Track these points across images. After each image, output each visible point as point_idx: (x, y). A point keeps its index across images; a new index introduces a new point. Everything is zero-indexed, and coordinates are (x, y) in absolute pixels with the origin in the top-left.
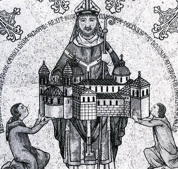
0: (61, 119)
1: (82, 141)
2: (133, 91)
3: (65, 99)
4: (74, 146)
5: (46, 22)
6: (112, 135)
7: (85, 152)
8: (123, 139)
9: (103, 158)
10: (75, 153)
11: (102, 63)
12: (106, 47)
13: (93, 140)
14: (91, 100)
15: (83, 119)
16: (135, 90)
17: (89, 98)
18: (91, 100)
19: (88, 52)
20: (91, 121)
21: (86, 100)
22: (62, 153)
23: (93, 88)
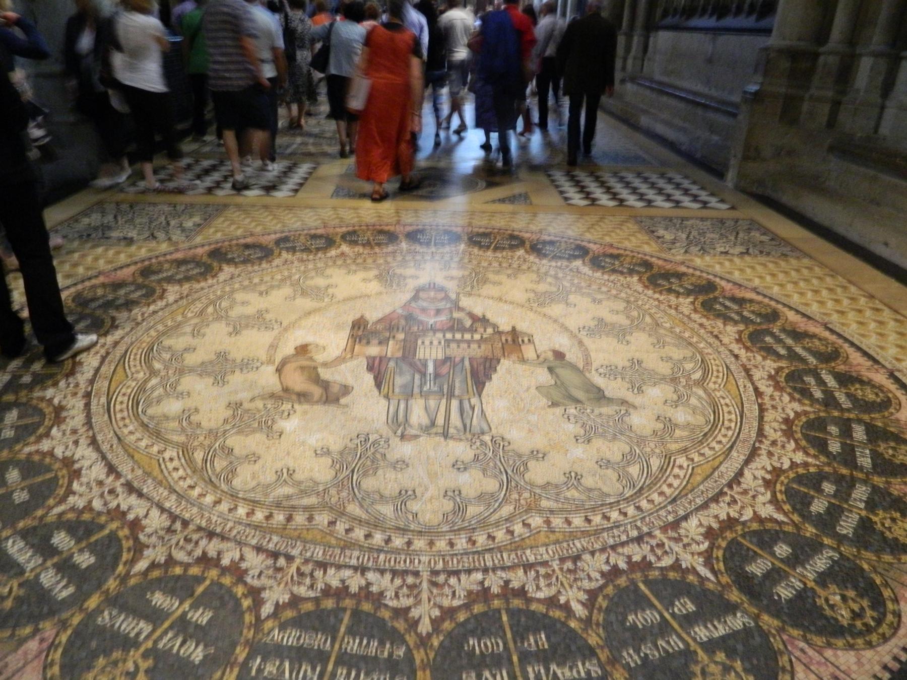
0: (381, 358)
1: (417, 377)
2: (507, 340)
3: (391, 342)
4: (399, 381)
5: (373, 292)
6: (474, 374)
7: (421, 386)
8: (494, 377)
9: (457, 392)
10: (404, 386)
11: (451, 318)
12: (460, 309)
13: (437, 375)
14: (435, 343)
15: (422, 357)
16: (510, 339)
17: (431, 343)
18: (435, 343)
19: (432, 313)
20: (435, 361)
21: (427, 343)
22: (378, 385)
23: (440, 335)
